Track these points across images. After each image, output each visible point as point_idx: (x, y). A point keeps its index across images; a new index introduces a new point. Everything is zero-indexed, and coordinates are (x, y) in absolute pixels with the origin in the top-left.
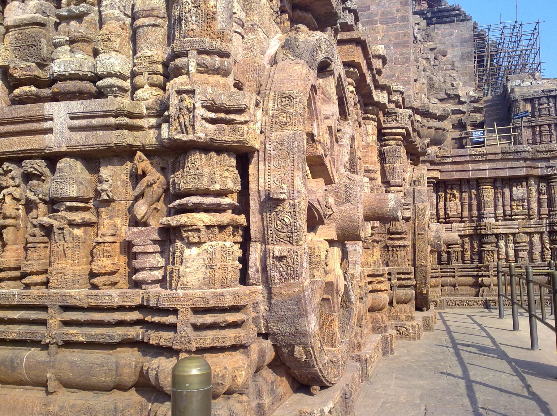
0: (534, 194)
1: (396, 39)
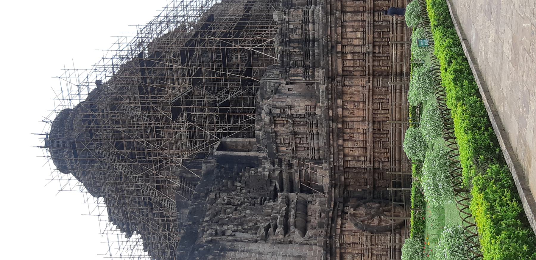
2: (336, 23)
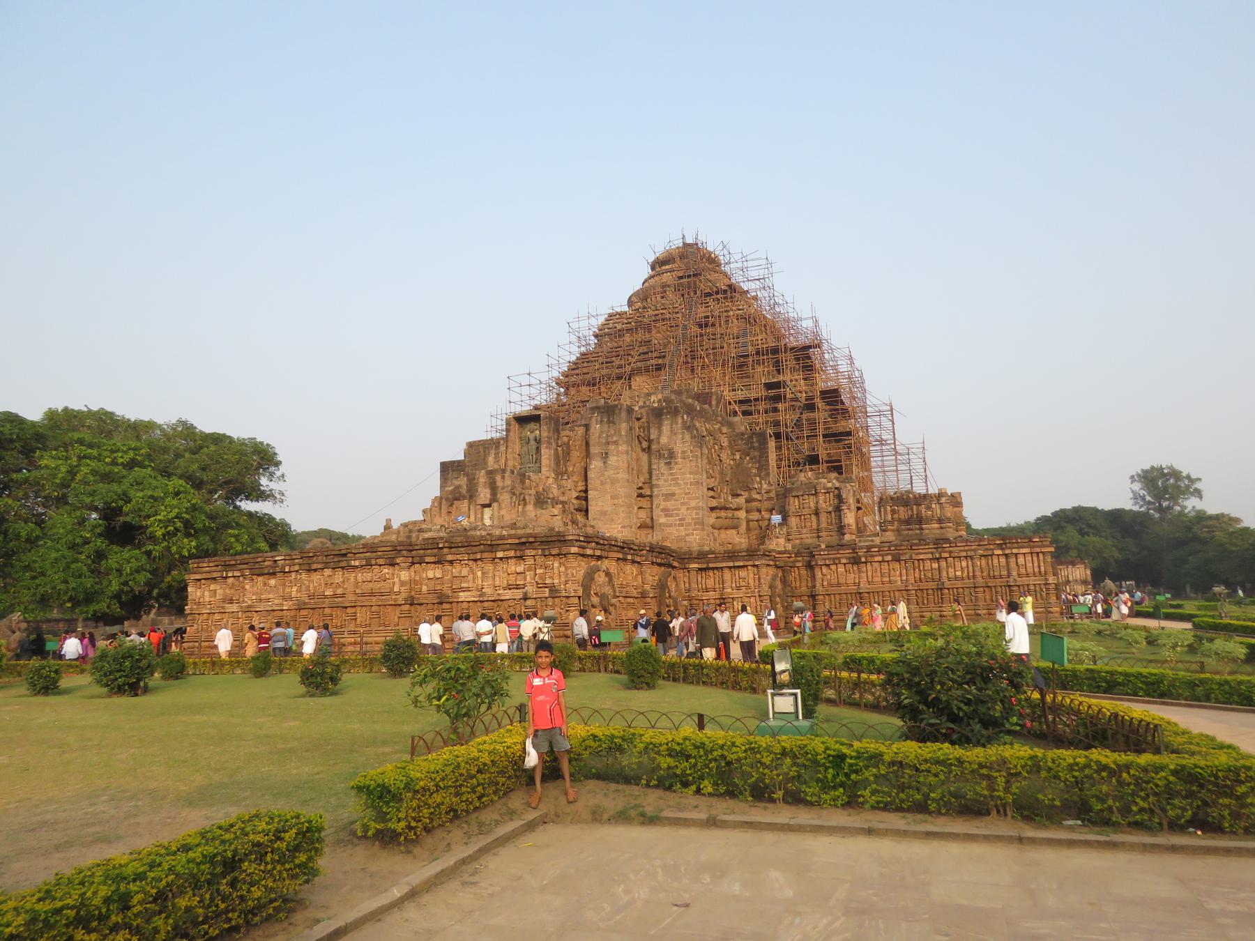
0: (751, 575)
2: (971, 550)
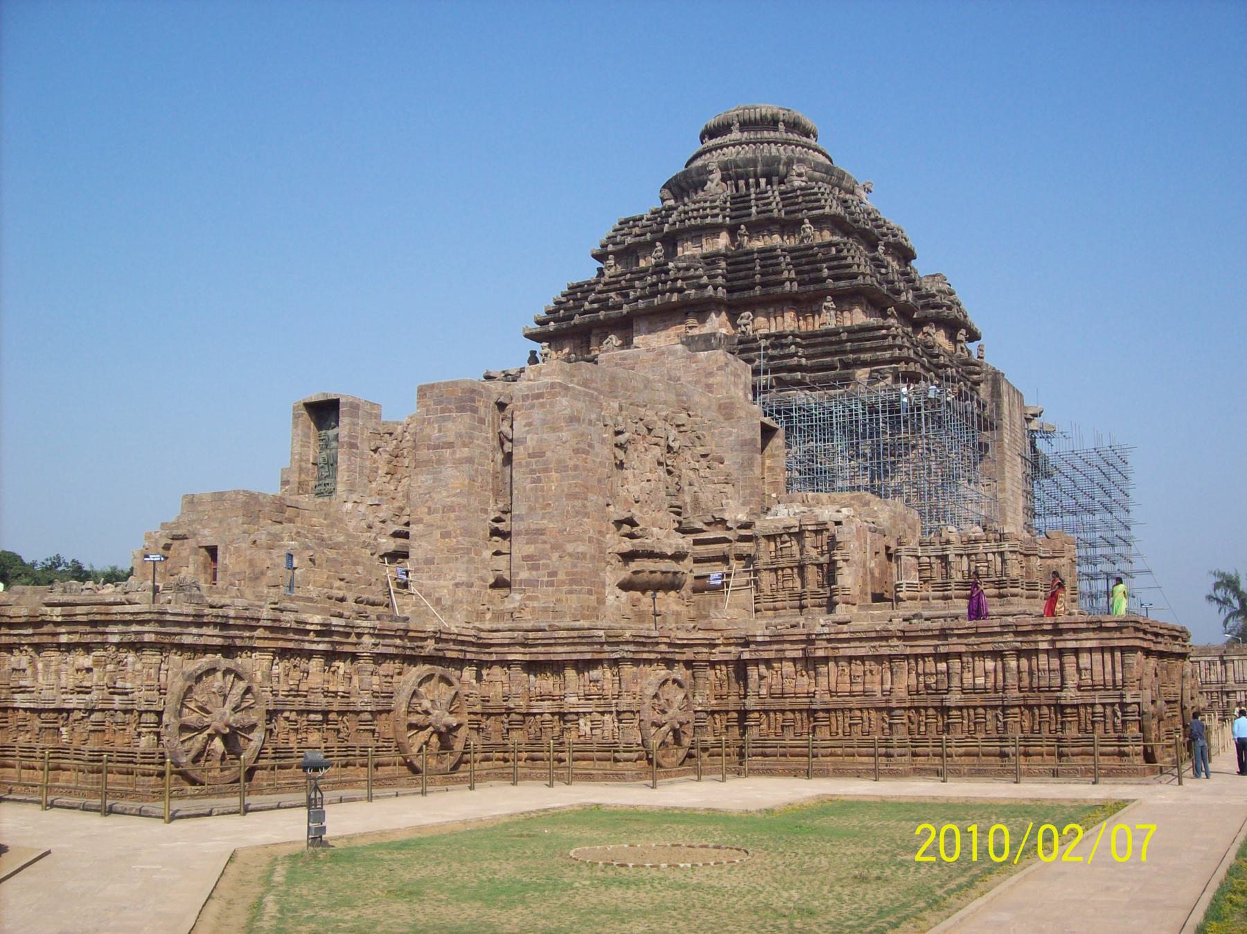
0: (608, 674)
1: (569, 489)
